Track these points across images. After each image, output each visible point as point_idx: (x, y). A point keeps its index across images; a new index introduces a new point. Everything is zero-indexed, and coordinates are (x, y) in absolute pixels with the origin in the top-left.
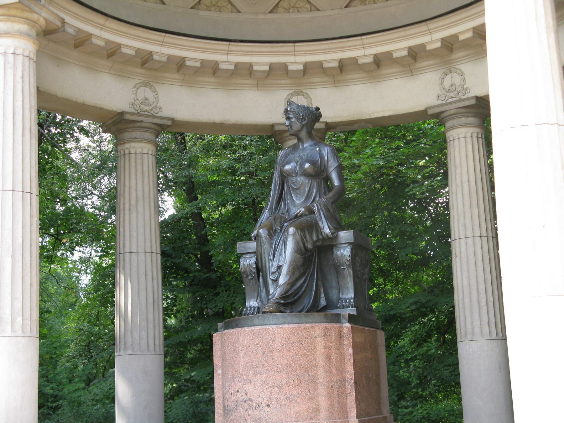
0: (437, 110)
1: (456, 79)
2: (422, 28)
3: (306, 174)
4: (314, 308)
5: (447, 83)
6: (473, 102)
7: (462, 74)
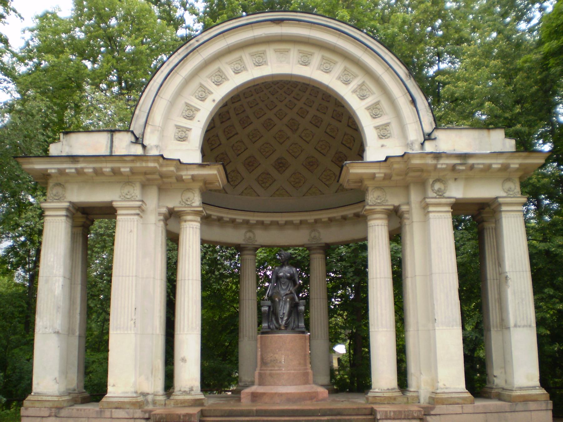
4: (293, 329)
5: (313, 235)
6: (323, 245)
7: (319, 233)
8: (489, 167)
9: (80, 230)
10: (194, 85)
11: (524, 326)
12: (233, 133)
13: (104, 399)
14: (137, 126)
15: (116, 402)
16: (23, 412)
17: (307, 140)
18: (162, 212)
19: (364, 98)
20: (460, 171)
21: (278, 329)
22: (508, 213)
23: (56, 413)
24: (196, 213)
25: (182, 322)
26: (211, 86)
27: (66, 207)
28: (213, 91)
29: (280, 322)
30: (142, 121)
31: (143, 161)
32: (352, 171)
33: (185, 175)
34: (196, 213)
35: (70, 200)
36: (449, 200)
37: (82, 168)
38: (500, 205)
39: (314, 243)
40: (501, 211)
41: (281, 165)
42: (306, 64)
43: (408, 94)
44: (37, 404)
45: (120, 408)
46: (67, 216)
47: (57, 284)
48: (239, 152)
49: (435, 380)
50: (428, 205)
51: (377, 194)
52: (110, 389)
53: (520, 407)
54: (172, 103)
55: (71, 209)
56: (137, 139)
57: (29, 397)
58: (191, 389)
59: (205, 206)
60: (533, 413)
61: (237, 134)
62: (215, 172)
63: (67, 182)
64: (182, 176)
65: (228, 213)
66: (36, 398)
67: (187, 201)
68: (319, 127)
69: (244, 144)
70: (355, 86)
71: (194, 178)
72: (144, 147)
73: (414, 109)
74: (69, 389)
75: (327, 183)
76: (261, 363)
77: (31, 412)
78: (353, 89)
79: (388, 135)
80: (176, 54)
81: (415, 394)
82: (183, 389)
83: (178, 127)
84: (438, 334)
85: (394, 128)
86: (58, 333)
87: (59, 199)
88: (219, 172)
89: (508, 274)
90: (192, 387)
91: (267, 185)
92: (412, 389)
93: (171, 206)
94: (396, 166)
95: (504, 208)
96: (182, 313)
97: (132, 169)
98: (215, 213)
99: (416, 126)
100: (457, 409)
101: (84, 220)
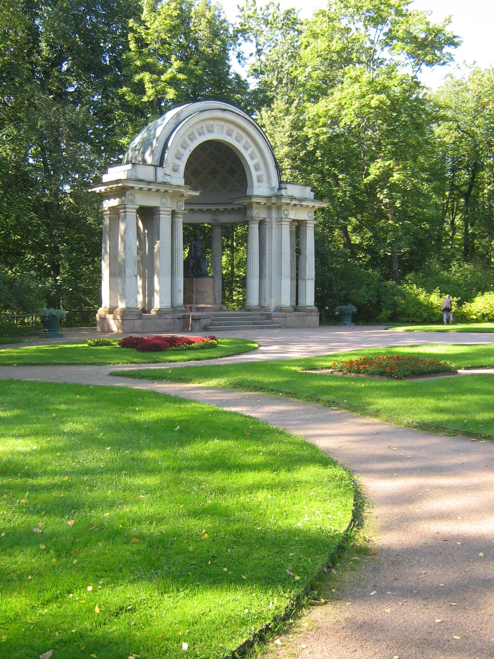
8: (307, 206)
53: (309, 314)
95: (308, 225)
100: (289, 314)
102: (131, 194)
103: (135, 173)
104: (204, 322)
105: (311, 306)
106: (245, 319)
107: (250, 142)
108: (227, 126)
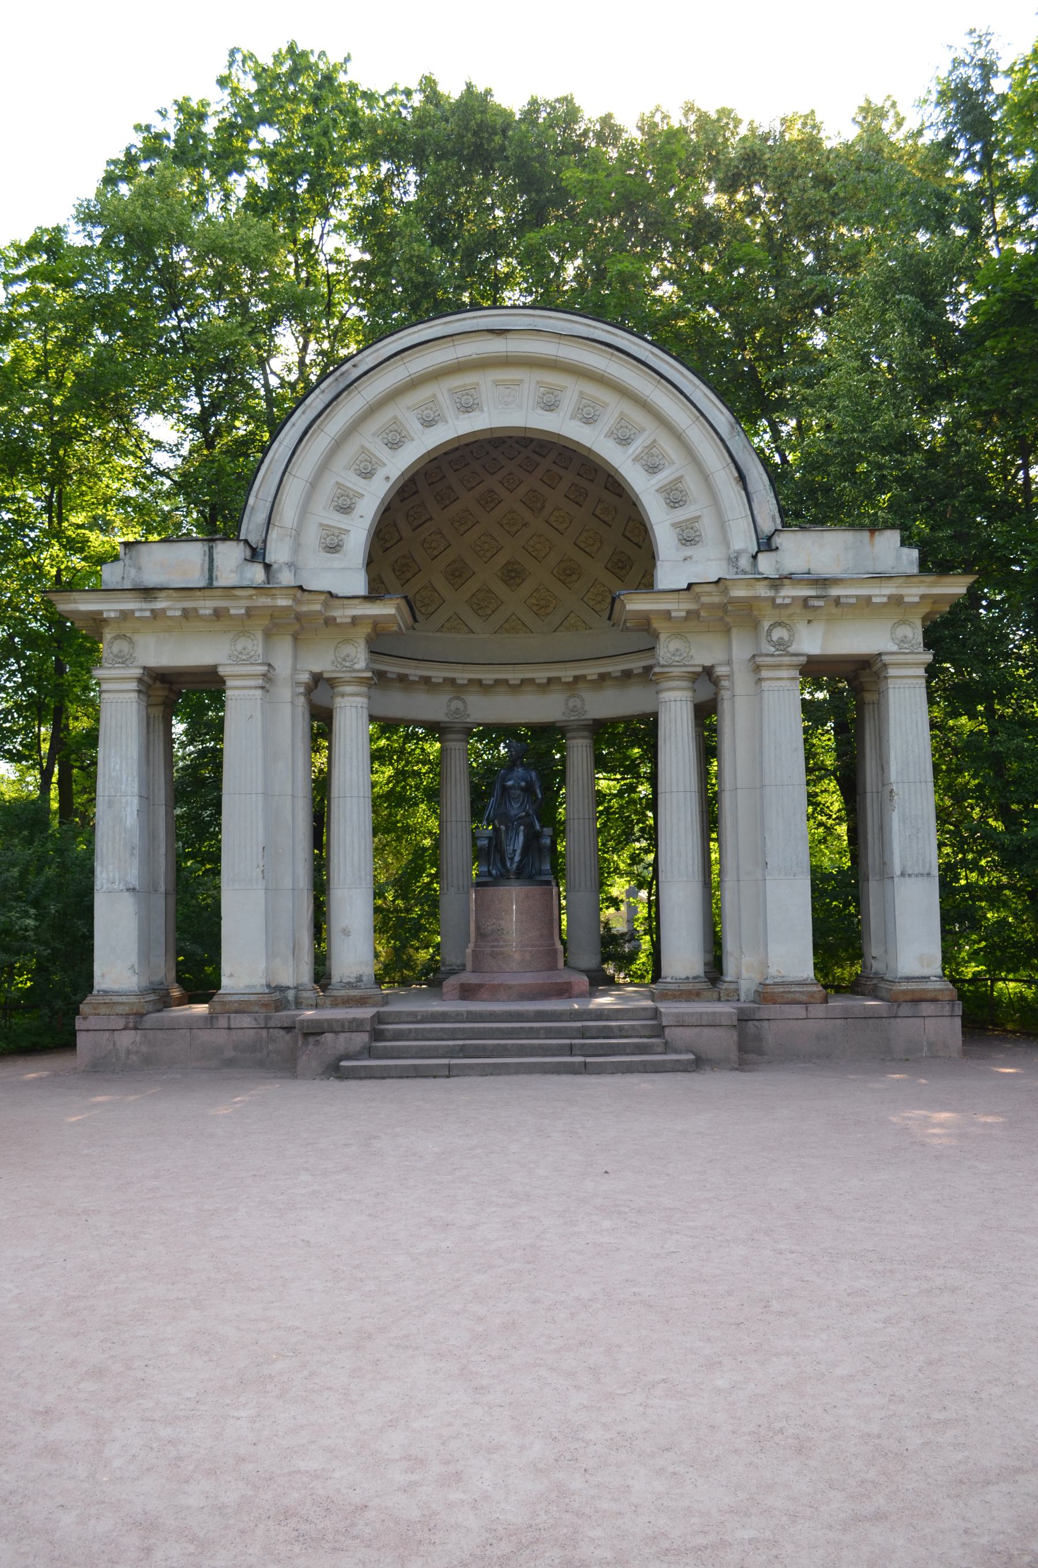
0: (562, 724)
1: (578, 703)
2: (561, 666)
3: (522, 789)
5: (571, 703)
6: (591, 722)
7: (583, 700)
9: (158, 711)
10: (350, 450)
11: (917, 875)
12: (424, 519)
13: (216, 998)
14: (251, 526)
15: (236, 1002)
16: (79, 1023)
17: (559, 527)
18: (302, 681)
19: (656, 470)
20: (816, 608)
21: (502, 877)
22: (899, 681)
23: (135, 1023)
24: (361, 681)
25: (342, 868)
26: (381, 452)
27: (138, 676)
28: (386, 461)
29: (508, 864)
30: (261, 516)
31: (267, 595)
32: (629, 607)
33: (340, 617)
34: (361, 681)
35: (144, 664)
36: (795, 658)
37: (164, 610)
38: (885, 666)
39: (572, 718)
40: (886, 678)
41: (513, 575)
42: (550, 407)
43: (732, 466)
44: (103, 1010)
45: (244, 1012)
46: (139, 691)
47: (129, 809)
48: (436, 553)
49: (765, 964)
50: (757, 668)
51: (675, 645)
52: (224, 981)
53: (905, 1009)
54: (314, 484)
55: (146, 678)
56: (254, 550)
57: (89, 999)
58: (360, 979)
59: (375, 657)
60: (927, 1020)
61: (431, 519)
62: (393, 611)
63: (135, 631)
64: (334, 619)
65: (416, 667)
66: (100, 1000)
67: (345, 660)
68: (581, 506)
69: (444, 538)
70: (640, 450)
71: (355, 620)
72: (268, 567)
73: (743, 493)
74: (151, 983)
75: (598, 608)
76: (477, 935)
77: (92, 1022)
78: (633, 457)
79: (697, 539)
80: (317, 391)
81: (732, 986)
82: (345, 980)
83: (323, 527)
84: (770, 885)
85: (708, 527)
86: (134, 889)
87: (124, 660)
88: (398, 608)
89: (894, 787)
90: (361, 976)
91: (488, 611)
92: (728, 979)
93: (317, 669)
94: (705, 599)
95: (892, 672)
96: (342, 854)
97: (248, 609)
98: (394, 668)
99: (746, 524)
100: (799, 1011)
101: (166, 693)
102: (118, 637)
103: (133, 572)
104: (334, 1043)
105: (925, 979)
106: (550, 1033)
107: (638, 416)
108: (530, 380)
